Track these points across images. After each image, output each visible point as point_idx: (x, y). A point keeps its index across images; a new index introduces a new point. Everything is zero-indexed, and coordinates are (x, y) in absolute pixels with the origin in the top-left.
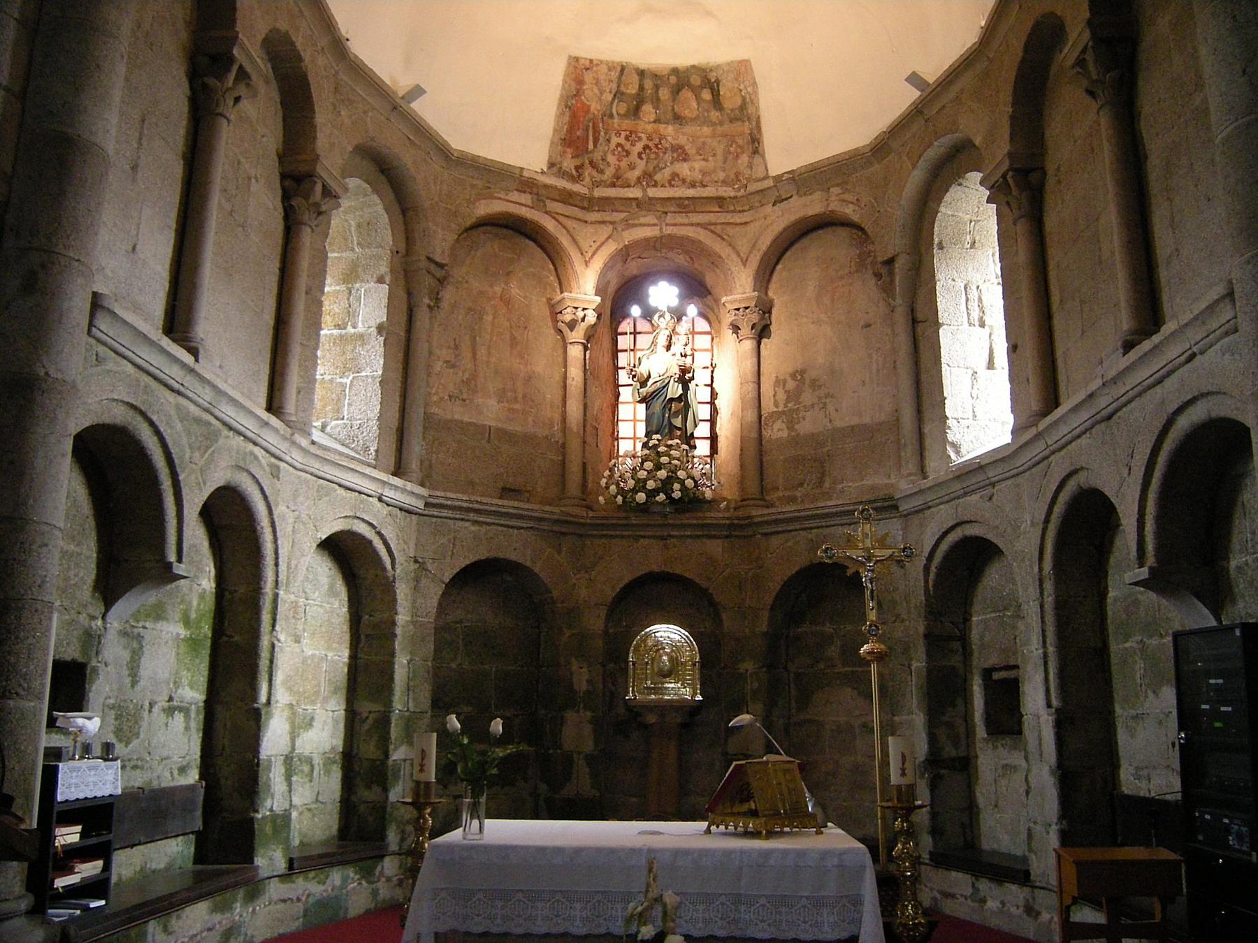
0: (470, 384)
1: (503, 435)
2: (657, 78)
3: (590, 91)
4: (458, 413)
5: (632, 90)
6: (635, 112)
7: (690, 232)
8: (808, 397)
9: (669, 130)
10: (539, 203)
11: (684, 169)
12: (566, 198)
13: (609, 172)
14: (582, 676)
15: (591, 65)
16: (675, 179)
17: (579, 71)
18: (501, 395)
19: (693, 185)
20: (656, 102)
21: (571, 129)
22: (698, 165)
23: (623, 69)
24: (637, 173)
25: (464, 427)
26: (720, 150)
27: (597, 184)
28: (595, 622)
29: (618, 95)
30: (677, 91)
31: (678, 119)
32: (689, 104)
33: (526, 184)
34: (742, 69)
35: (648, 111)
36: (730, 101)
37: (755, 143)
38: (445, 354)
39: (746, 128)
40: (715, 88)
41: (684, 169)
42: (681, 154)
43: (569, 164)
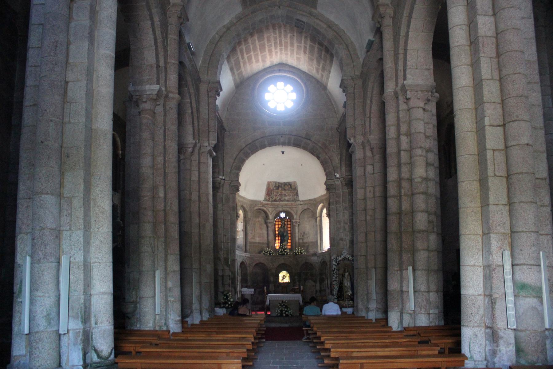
0: (254, 236)
1: (259, 243)
2: (281, 184)
3: (270, 186)
4: (253, 241)
5: (277, 185)
6: (278, 189)
7: (287, 209)
8: (305, 236)
9: (283, 191)
10: (263, 206)
11: (286, 198)
12: (267, 204)
13: (274, 199)
14: (272, 279)
15: (271, 182)
16: (284, 200)
17: (269, 184)
18: (259, 237)
19: (287, 201)
20: (281, 187)
21: (268, 192)
22: (288, 197)
23: (276, 182)
24: (278, 199)
25: (254, 243)
26: (292, 194)
27: (271, 201)
28: (274, 271)
29: (275, 186)
30: (284, 186)
31: (285, 190)
32: (287, 188)
33: (261, 203)
34: (295, 183)
35: (280, 189)
36: (293, 187)
37: (297, 194)
38: (251, 231)
39: (296, 191)
40: (291, 185)
41: (286, 198)
42: (285, 195)
43: (267, 198)
